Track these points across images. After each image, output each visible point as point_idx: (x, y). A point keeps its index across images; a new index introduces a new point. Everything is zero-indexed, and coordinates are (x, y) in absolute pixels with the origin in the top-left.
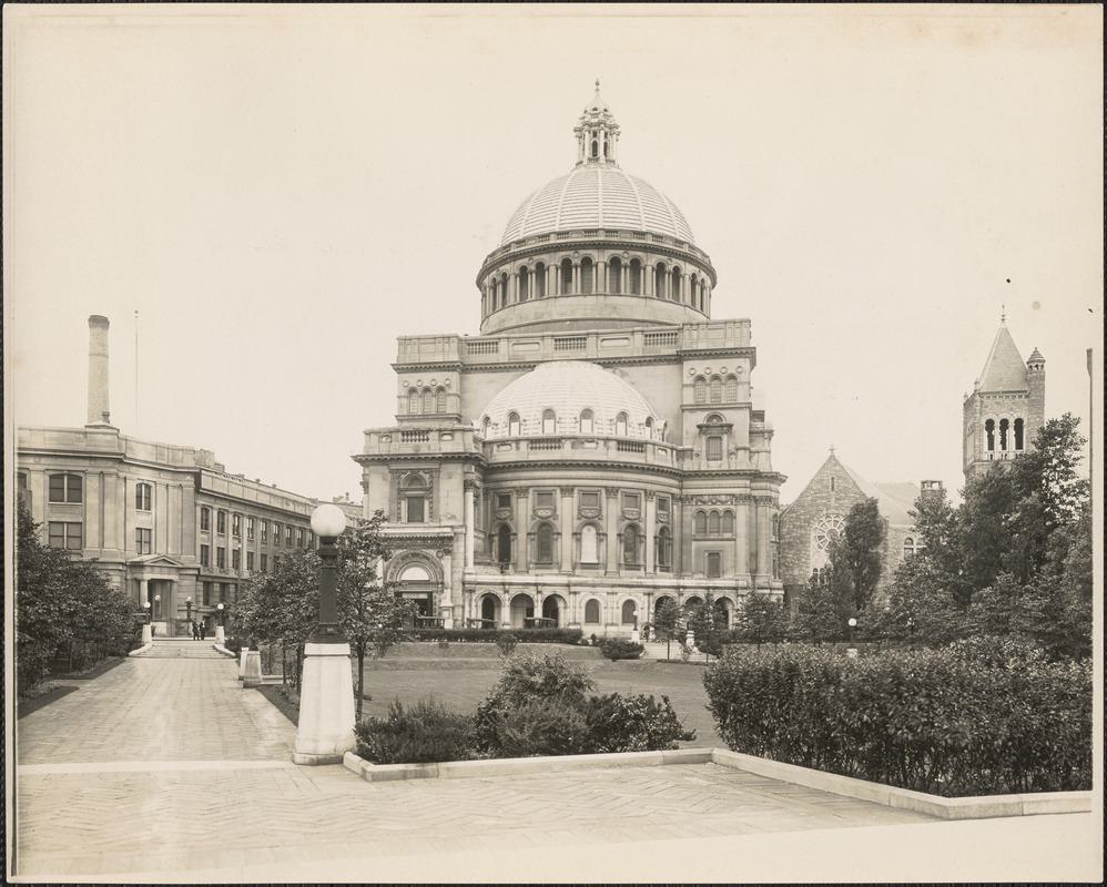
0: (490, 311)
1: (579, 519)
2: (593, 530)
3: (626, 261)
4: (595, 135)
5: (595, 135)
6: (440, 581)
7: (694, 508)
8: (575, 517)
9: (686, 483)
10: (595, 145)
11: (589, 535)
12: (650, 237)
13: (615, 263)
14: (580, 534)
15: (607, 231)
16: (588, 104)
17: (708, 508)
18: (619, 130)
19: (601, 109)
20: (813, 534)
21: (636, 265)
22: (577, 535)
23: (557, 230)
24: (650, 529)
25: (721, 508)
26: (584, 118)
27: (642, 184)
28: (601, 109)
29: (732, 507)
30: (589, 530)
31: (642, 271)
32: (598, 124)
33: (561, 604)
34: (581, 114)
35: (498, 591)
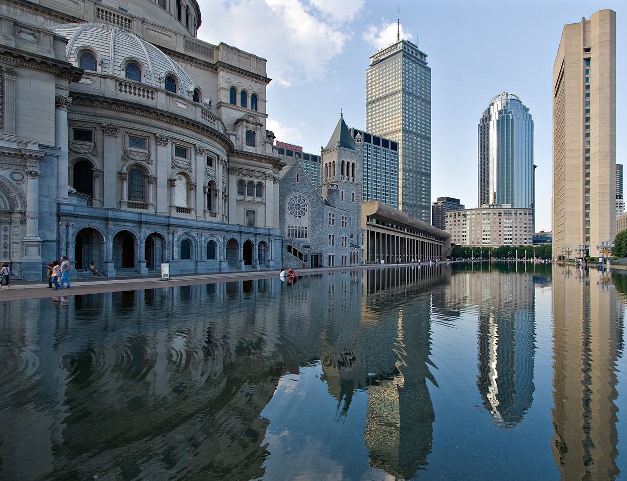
1: (173, 168)
2: (184, 180)
6: (19, 208)
7: (239, 177)
8: (170, 166)
9: (231, 158)
11: (181, 186)
14: (175, 180)
17: (247, 179)
20: (287, 206)
22: (171, 183)
24: (220, 186)
25: (256, 181)
29: (263, 181)
30: (180, 179)
33: (158, 243)
35: (97, 225)
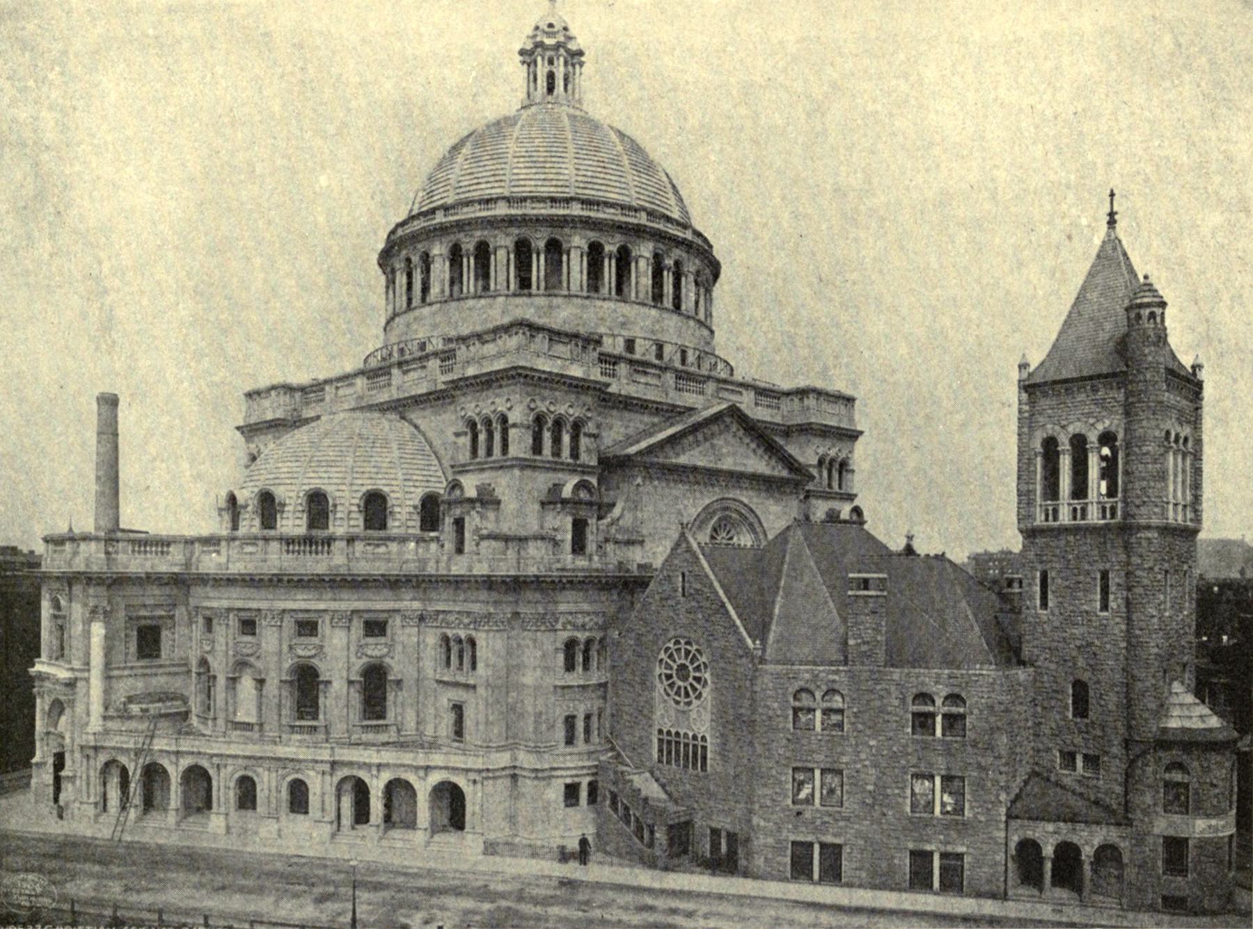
0: (402, 301)
3: (610, 248)
4: (551, 62)
5: (551, 62)
10: (551, 77)
12: (644, 215)
13: (595, 252)
15: (583, 202)
16: (536, 14)
18: (583, 59)
19: (558, 27)
21: (624, 260)
23: (507, 194)
26: (535, 36)
27: (621, 135)
28: (558, 27)
31: (633, 265)
32: (558, 46)
34: (531, 33)
